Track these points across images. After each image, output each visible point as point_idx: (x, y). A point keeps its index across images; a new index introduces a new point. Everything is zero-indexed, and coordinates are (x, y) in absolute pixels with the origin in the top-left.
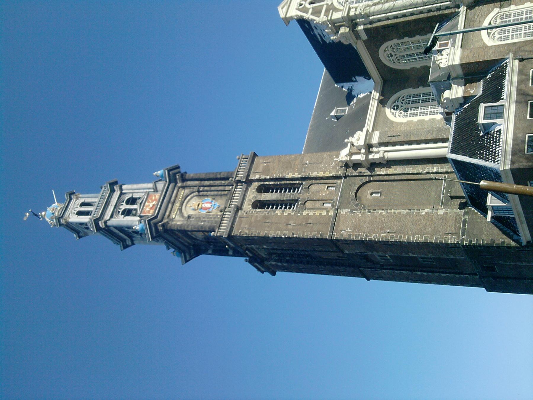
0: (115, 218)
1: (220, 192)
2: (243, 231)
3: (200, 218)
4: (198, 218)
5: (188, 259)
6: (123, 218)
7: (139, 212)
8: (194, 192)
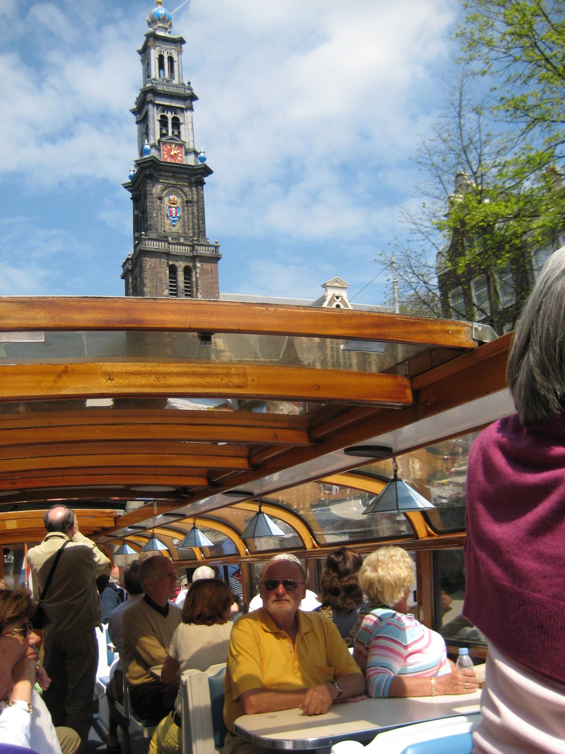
1: (187, 224)
3: (160, 210)
4: (160, 209)
7: (164, 139)
8: (186, 195)
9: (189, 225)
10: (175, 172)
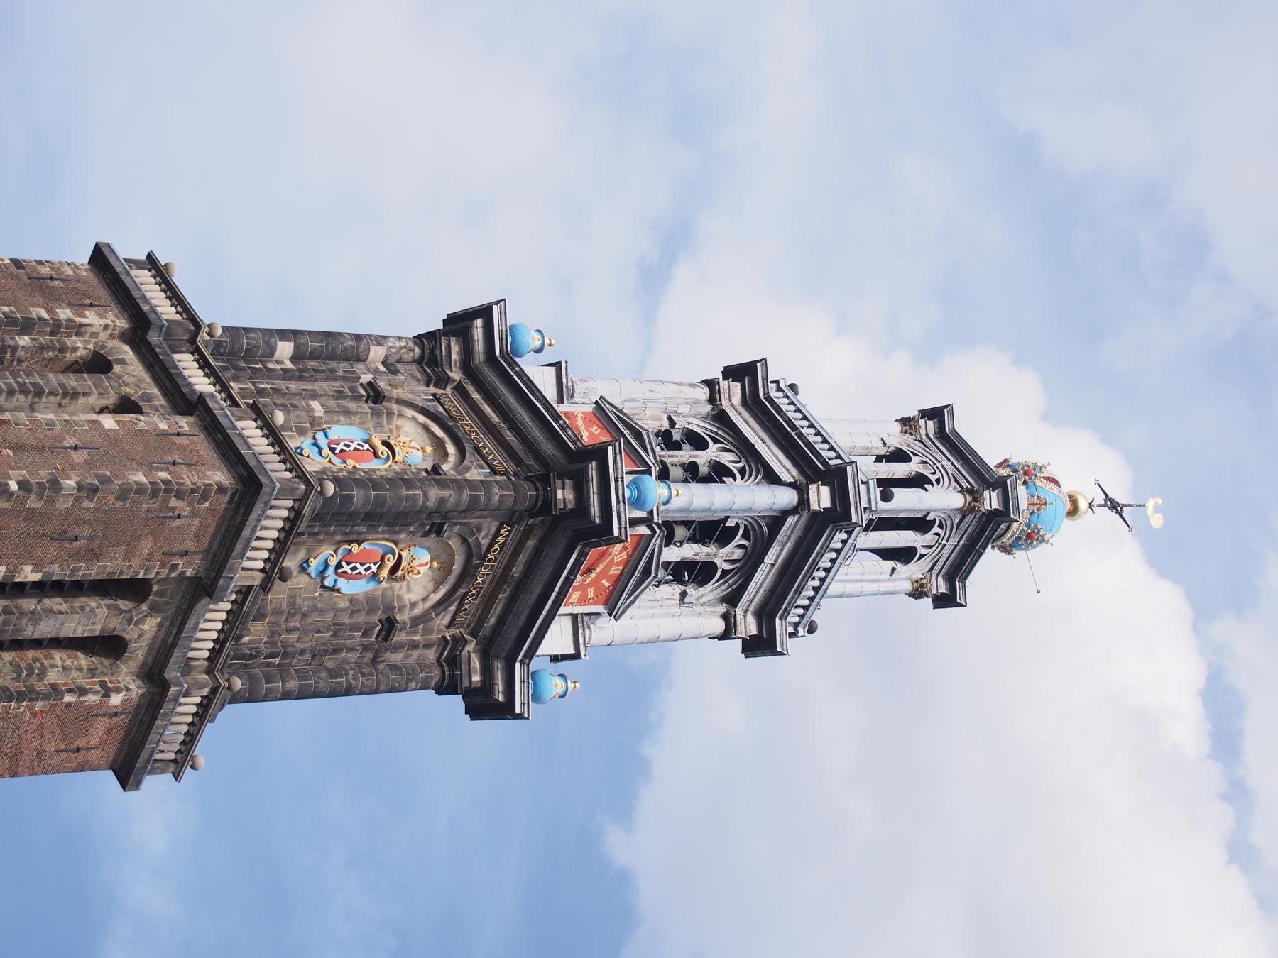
0: (764, 517)
2: (190, 504)
5: (479, 323)
6: (727, 518)
9: (289, 631)
10: (521, 586)
